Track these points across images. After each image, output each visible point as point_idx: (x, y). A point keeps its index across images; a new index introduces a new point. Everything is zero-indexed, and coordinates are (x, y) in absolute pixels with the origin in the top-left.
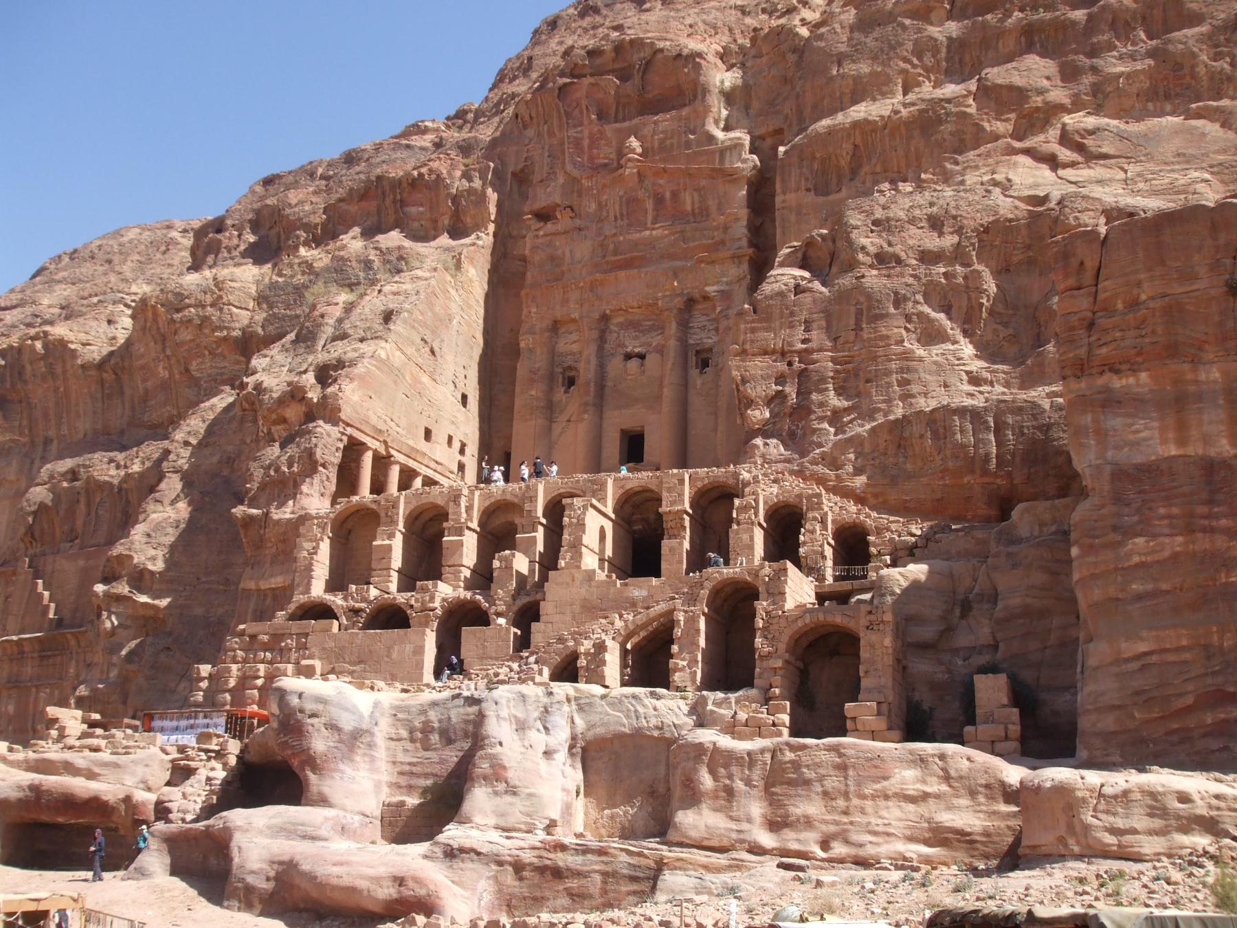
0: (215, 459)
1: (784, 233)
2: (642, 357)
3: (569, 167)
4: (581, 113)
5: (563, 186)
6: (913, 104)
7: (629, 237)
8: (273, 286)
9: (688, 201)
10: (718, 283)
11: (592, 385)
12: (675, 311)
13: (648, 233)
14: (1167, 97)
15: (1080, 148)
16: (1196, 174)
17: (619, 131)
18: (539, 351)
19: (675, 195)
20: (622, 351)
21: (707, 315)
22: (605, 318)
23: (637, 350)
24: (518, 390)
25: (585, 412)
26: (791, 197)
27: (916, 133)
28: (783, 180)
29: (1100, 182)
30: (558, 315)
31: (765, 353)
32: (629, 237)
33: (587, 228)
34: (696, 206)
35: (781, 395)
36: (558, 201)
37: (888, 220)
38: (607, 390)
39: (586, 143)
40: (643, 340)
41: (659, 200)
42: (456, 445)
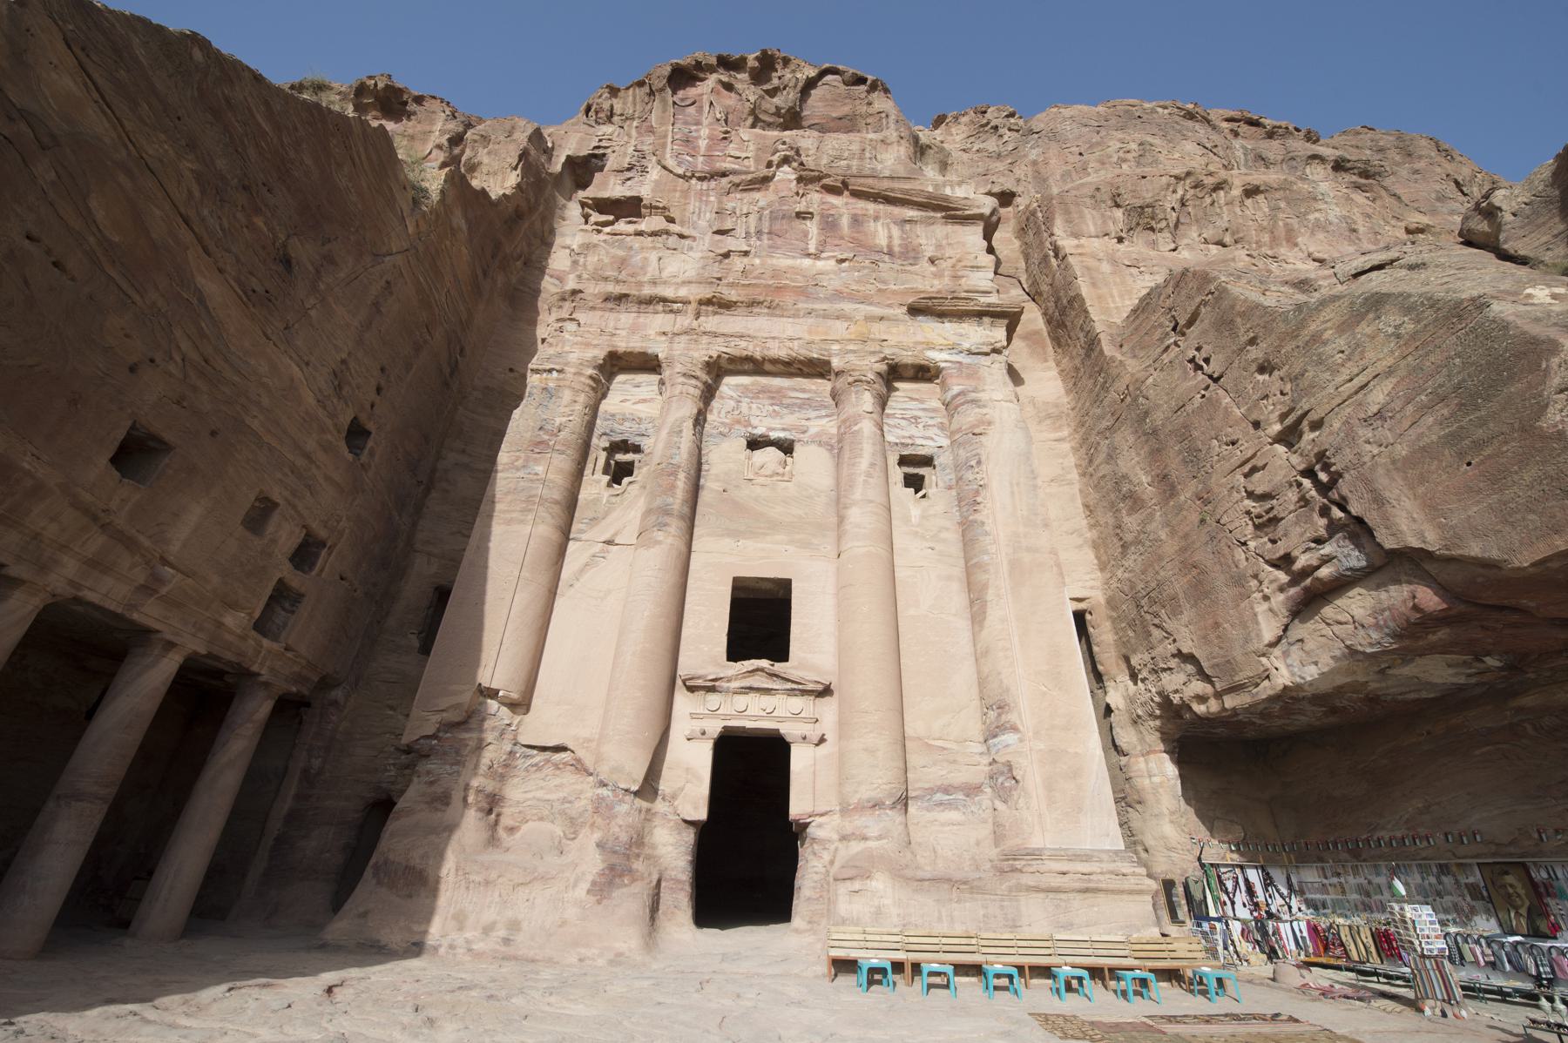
1: (1094, 285)
2: (787, 448)
3: (670, 163)
5: (656, 182)
7: (774, 261)
10: (952, 348)
11: (682, 476)
12: (871, 376)
13: (807, 262)
18: (567, 395)
19: (856, 221)
21: (921, 401)
22: (718, 369)
23: (774, 435)
24: (503, 457)
25: (662, 526)
27: (1283, 204)
28: (1069, 221)
30: (622, 345)
32: (769, 261)
33: (694, 239)
34: (896, 242)
38: (705, 496)
40: (791, 419)
41: (830, 225)
42: (284, 535)
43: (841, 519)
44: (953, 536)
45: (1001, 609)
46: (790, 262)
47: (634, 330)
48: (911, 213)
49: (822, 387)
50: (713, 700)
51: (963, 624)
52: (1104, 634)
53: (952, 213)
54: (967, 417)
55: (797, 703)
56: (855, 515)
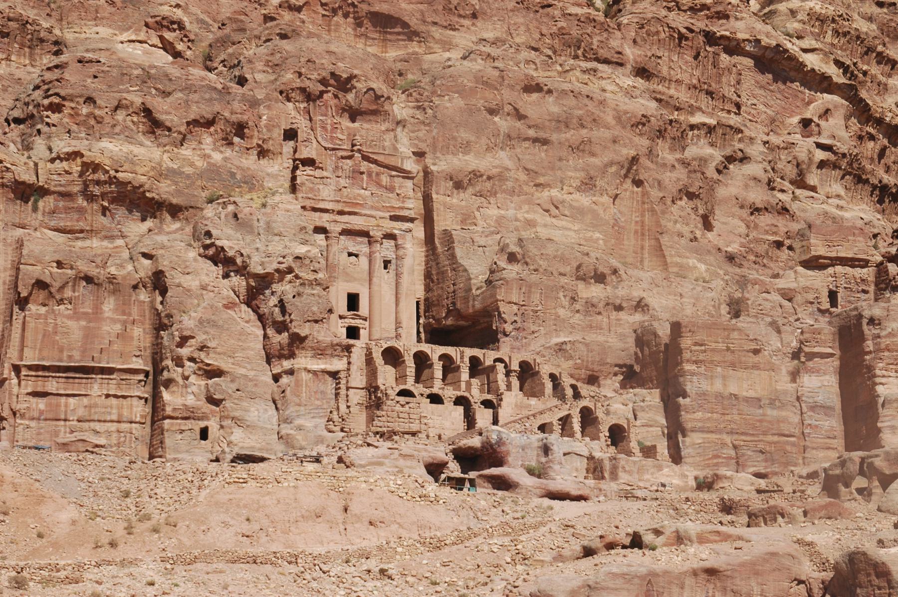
0: (197, 283)
3: (320, 139)
4: (326, 108)
6: (496, 167)
8: (168, 169)
9: (385, 179)
10: (401, 230)
14: (584, 191)
15: (557, 208)
16: (598, 235)
17: (348, 128)
20: (346, 251)
26: (441, 198)
29: (567, 229)
31: (510, 303)
35: (515, 321)
36: (314, 157)
37: (547, 255)
39: (329, 127)
40: (358, 248)
41: (370, 175)
43: (370, 280)
44: (394, 284)
45: (402, 304)
46: (358, 191)
47: (320, 218)
48: (394, 173)
49: (366, 240)
50: (346, 320)
51: (394, 306)
52: (422, 307)
53: (407, 175)
54: (401, 252)
55: (361, 321)
56: (375, 280)
